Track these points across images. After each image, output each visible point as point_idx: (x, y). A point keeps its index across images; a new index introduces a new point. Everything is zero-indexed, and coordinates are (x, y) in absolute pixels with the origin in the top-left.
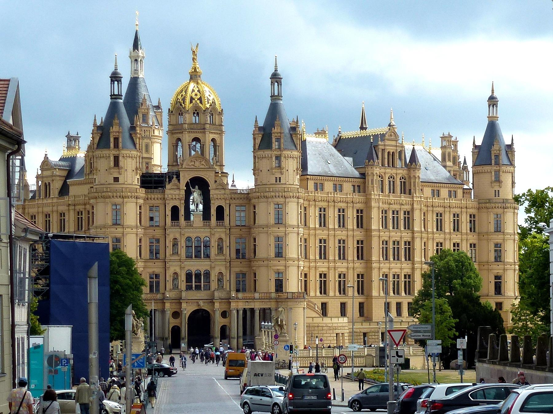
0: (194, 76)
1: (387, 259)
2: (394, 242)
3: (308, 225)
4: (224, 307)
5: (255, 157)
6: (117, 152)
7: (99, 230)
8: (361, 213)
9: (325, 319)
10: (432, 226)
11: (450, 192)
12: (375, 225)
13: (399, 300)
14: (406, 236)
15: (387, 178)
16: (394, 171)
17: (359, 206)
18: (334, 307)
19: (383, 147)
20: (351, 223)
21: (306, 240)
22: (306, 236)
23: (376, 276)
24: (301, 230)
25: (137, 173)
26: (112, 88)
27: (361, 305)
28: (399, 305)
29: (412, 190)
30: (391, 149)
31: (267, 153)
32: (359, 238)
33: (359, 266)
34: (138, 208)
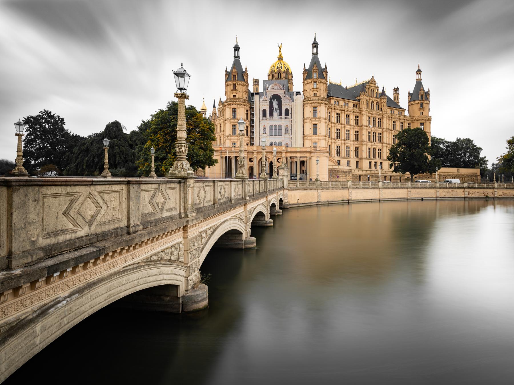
0: (280, 58)
1: (370, 141)
2: (373, 133)
3: (331, 121)
4: (279, 156)
5: (304, 85)
6: (235, 82)
7: (227, 121)
8: (358, 118)
9: (339, 166)
10: (391, 127)
11: (399, 112)
12: (365, 123)
13: (376, 161)
14: (380, 130)
15: (370, 102)
16: (374, 99)
17: (357, 114)
18: (344, 162)
19: (369, 87)
20: (353, 121)
21: (330, 128)
22: (330, 127)
23: (365, 149)
24: (327, 122)
25: (245, 93)
26: (235, 53)
27: (357, 162)
28: (376, 163)
29: (382, 109)
30: (373, 88)
31: (310, 80)
32: (356, 130)
33: (357, 144)
34: (246, 111)
